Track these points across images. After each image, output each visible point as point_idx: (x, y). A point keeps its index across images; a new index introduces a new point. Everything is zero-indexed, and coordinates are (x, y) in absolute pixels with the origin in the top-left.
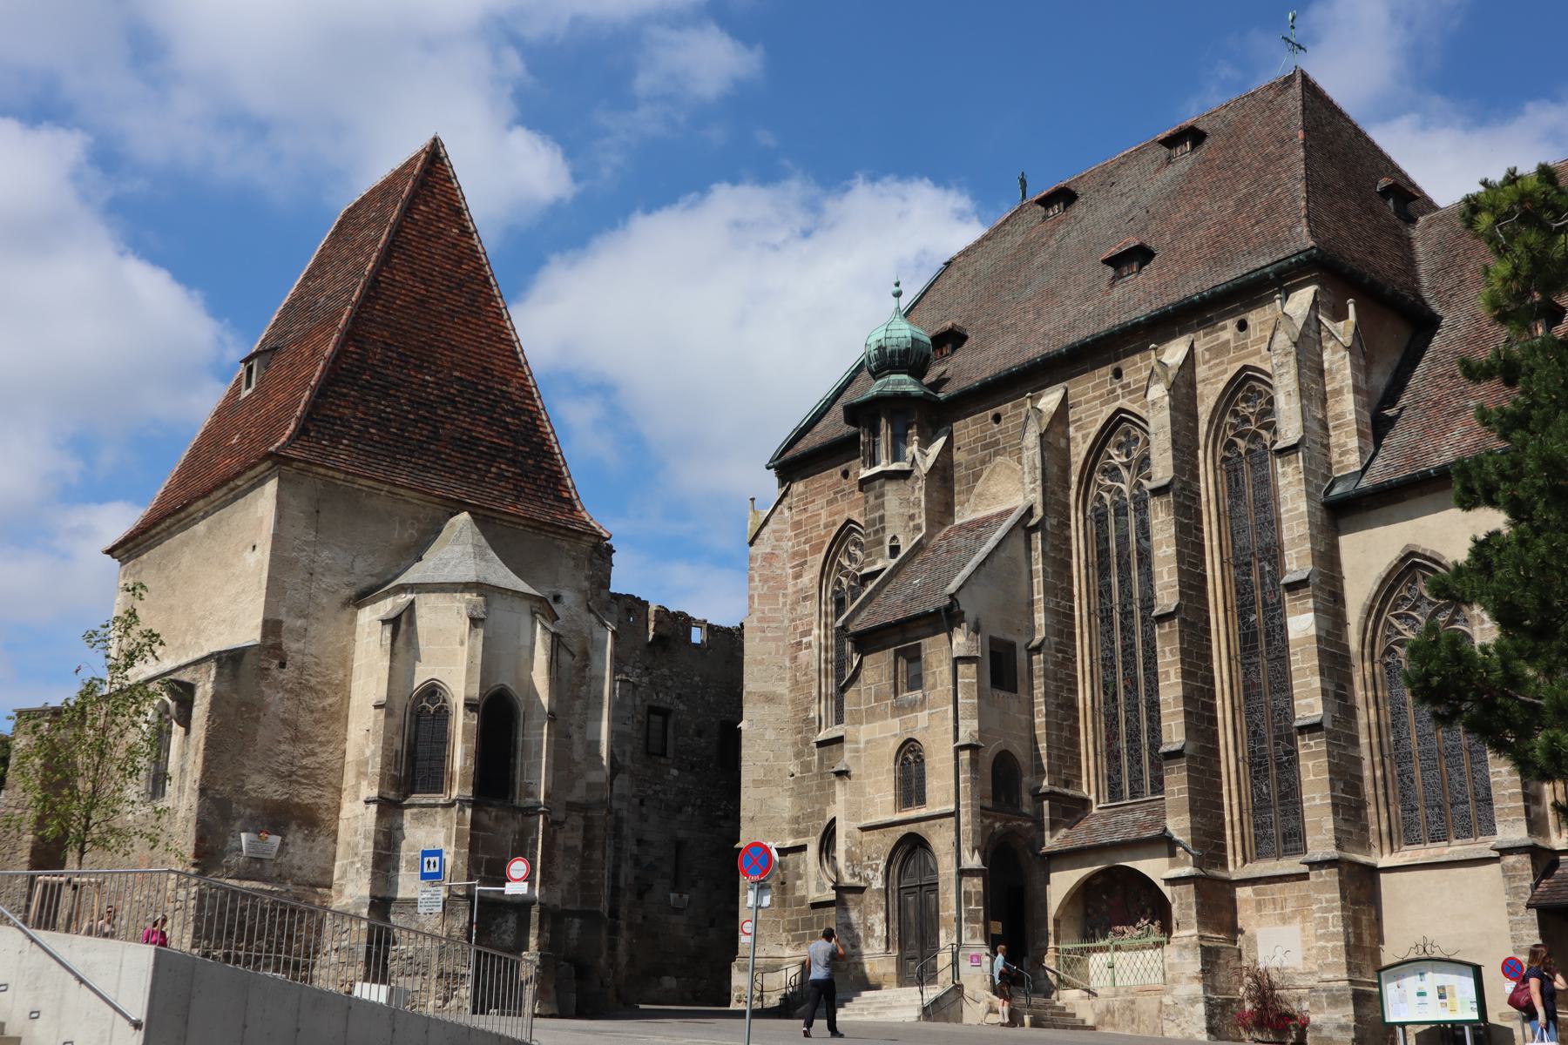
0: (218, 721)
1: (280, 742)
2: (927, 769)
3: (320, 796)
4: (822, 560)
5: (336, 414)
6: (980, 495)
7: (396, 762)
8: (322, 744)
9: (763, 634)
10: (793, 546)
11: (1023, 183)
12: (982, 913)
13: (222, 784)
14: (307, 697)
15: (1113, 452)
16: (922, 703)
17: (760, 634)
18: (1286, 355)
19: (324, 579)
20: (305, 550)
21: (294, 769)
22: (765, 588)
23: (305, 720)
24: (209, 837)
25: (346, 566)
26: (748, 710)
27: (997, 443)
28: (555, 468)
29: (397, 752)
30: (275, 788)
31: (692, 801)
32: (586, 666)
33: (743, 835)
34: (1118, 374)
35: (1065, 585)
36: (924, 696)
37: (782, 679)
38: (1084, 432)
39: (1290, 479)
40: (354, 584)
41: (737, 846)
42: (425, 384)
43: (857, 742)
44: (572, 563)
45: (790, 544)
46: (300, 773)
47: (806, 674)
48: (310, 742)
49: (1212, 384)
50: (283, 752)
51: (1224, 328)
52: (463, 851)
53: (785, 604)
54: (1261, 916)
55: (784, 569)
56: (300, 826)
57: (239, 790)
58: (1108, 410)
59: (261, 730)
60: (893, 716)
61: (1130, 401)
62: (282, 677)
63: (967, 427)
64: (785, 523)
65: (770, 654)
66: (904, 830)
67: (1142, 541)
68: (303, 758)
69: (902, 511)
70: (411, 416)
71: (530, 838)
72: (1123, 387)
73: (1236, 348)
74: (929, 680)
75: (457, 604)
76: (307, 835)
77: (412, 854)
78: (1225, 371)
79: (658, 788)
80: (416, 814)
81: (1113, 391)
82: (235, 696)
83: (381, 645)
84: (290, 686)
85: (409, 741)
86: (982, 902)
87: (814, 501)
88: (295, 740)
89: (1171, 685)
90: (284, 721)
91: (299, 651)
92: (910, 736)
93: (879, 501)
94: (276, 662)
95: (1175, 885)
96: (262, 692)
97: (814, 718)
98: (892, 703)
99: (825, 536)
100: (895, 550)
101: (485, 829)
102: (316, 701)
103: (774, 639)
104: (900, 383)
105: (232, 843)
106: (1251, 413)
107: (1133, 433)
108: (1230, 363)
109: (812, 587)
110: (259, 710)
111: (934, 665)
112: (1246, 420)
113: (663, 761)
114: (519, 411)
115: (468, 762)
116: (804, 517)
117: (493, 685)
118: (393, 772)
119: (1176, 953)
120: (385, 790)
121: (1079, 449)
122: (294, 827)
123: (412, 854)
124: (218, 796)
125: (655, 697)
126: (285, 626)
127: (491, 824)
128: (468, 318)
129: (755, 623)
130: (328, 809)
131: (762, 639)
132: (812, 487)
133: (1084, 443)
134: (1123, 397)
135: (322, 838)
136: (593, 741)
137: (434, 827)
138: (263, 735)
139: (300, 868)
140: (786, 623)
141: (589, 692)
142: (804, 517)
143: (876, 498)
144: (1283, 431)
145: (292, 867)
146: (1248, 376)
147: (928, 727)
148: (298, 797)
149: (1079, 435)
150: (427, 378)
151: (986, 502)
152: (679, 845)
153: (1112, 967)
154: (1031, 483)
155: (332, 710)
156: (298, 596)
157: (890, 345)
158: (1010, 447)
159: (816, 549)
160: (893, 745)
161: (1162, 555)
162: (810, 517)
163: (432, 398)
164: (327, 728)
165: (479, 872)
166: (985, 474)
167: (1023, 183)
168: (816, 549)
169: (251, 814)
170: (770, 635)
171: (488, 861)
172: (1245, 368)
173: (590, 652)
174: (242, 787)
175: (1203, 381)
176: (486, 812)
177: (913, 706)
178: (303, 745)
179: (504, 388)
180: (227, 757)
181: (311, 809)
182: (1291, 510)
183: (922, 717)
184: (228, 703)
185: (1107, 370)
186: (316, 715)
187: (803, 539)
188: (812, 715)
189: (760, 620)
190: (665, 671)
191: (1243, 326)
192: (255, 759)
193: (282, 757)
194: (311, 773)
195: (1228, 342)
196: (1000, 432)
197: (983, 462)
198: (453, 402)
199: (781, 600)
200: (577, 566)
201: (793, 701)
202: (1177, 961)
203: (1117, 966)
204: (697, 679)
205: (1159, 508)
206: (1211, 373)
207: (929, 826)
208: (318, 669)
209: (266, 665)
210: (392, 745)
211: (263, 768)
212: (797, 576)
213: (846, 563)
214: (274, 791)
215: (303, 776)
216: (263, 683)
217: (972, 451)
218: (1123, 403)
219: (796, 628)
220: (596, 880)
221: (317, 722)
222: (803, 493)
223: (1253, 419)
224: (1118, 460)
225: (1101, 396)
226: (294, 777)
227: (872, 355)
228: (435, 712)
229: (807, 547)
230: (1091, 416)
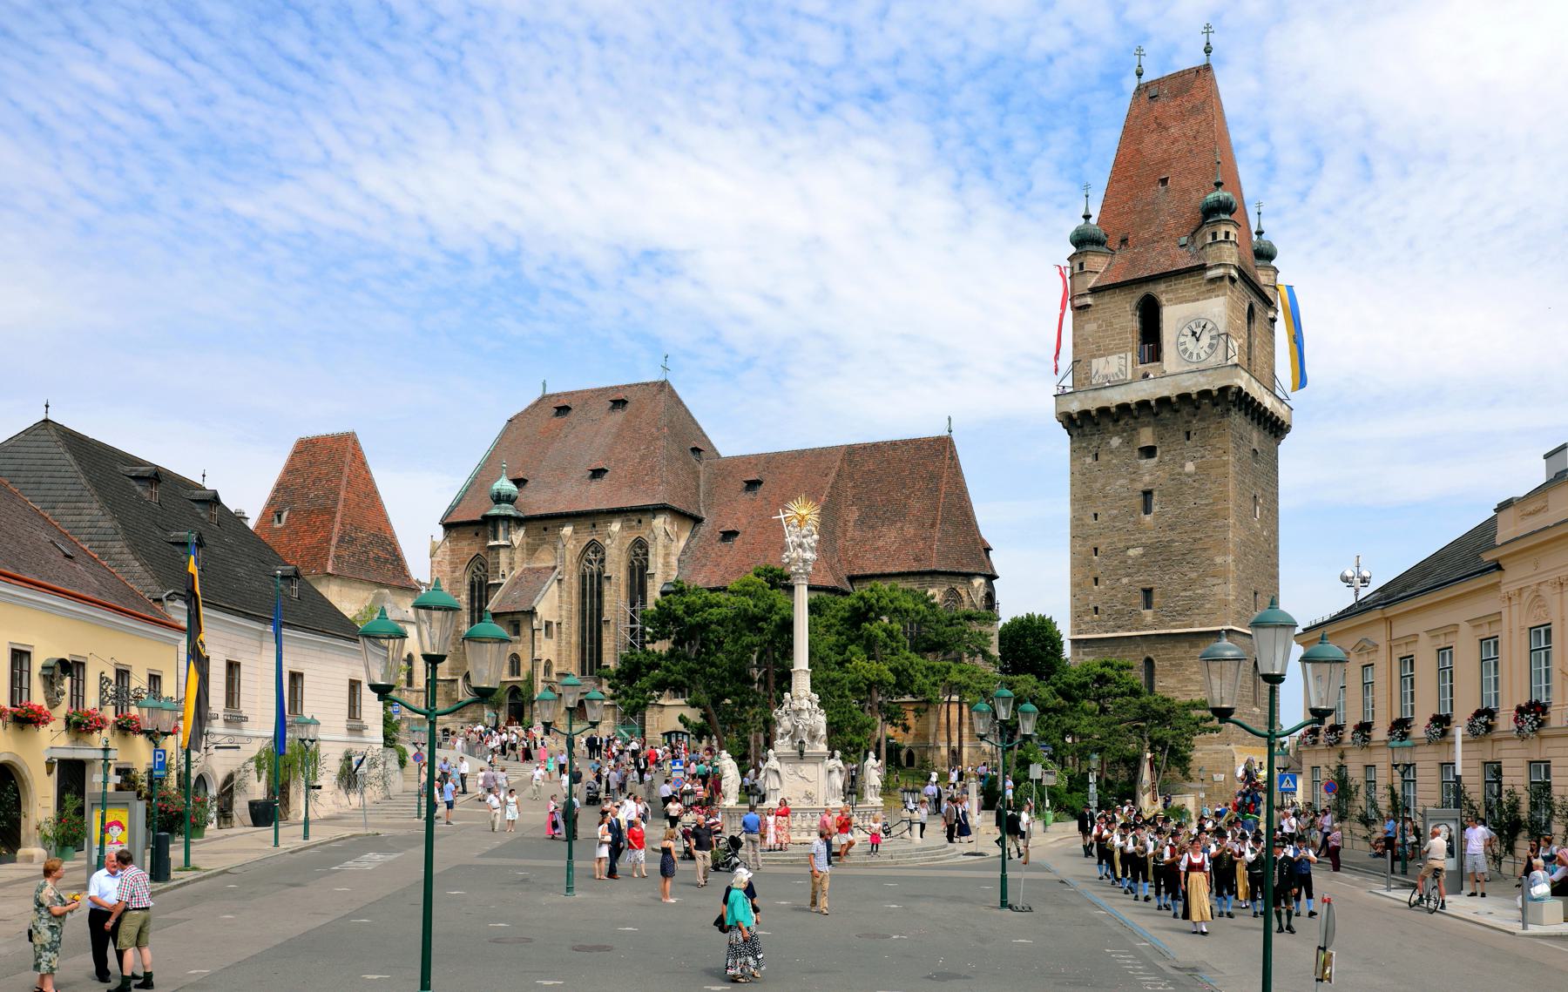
11: (544, 384)
34: (594, 526)
58: (590, 539)
74: (522, 634)
100: (503, 575)
104: (506, 508)
112: (638, 555)
159: (462, 562)
167: (544, 384)
168: (462, 562)
183: (520, 647)
191: (640, 522)
212: (453, 572)
218: (595, 537)
224: (592, 557)
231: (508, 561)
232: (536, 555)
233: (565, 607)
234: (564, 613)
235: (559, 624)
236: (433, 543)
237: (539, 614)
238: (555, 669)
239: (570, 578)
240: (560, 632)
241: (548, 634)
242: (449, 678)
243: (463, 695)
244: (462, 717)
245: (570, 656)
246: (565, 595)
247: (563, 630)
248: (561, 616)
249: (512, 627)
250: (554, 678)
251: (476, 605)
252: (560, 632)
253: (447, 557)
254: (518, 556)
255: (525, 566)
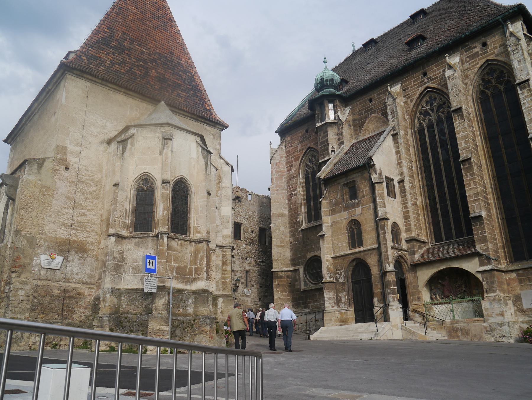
0: (28, 195)
1: (65, 208)
2: (363, 231)
3: (88, 237)
4: (299, 163)
5: (98, 55)
6: (365, 130)
7: (126, 215)
8: (89, 210)
9: (277, 192)
10: (287, 160)
12: (396, 290)
13: (31, 229)
14: (81, 186)
15: (424, 105)
16: (358, 205)
17: (276, 192)
18: (516, 46)
19: (90, 129)
20: (80, 114)
21: (73, 222)
22: (278, 175)
23: (80, 198)
24: (22, 257)
25: (102, 124)
26: (273, 220)
27: (372, 109)
28: (203, 97)
29: (126, 210)
30: (62, 232)
31: (251, 256)
32: (220, 182)
33: (274, 266)
34: (425, 74)
35: (409, 157)
36: (359, 201)
37: (285, 208)
38: (411, 99)
39: (526, 94)
40: (107, 133)
41: (272, 270)
42: (142, 53)
43: (328, 223)
44: (212, 137)
45: (286, 159)
46: (76, 224)
47: (295, 205)
48: (82, 209)
49: (472, 70)
50: (67, 213)
51: (475, 47)
52: (163, 261)
53: (285, 181)
54: (522, 286)
55: (284, 168)
56: (76, 252)
57: (42, 232)
58: (421, 89)
59: (54, 201)
60: (344, 211)
61: (431, 83)
62: (66, 175)
63: (357, 106)
64: (283, 152)
65: (280, 199)
66: (353, 257)
67: (442, 138)
68: (78, 217)
69: (335, 137)
70: (136, 64)
71: (199, 255)
72: (428, 79)
73: (482, 54)
75: (157, 135)
76: (81, 257)
77: (135, 264)
78: (478, 64)
79: (239, 251)
80: (137, 242)
81: (424, 80)
82: (40, 183)
83: (117, 155)
84: (71, 180)
85: (133, 204)
86: (396, 285)
87: (294, 142)
88: (74, 207)
89: (472, 189)
90: (68, 197)
91: (76, 163)
92: (353, 218)
93: (325, 134)
94: (64, 167)
95: (483, 274)
96: (55, 181)
97: (299, 221)
98: (343, 206)
99: (300, 154)
101: (175, 250)
102: (86, 189)
103: (282, 193)
105: (36, 261)
106: (491, 79)
107: (433, 96)
108: (479, 60)
109: (296, 173)
110: (53, 191)
111: (362, 188)
113: (240, 241)
114: (185, 72)
115: (165, 213)
116: (291, 148)
117: (178, 175)
118: (124, 220)
119: (488, 304)
120: (119, 229)
121: (409, 105)
122: (73, 252)
123: (135, 264)
124: (28, 235)
125: (236, 219)
126: (68, 149)
127: (179, 248)
128: (163, 31)
129: (274, 188)
130: (93, 243)
131: (277, 194)
132: (294, 138)
133: (411, 103)
134: (428, 82)
135: (89, 258)
136: (225, 216)
137: (147, 249)
138: (56, 203)
139: (77, 274)
140: (286, 187)
141: (222, 194)
142: (291, 148)
143: (324, 133)
144: (518, 77)
145: (73, 274)
146: (489, 63)
147: (361, 214)
148: (76, 237)
149: (409, 100)
150: (144, 50)
151: (368, 132)
152: (247, 272)
153: (452, 311)
154: (392, 118)
155: (95, 193)
156: (76, 136)
157: (325, 78)
158: (377, 110)
159: (296, 160)
160: (345, 223)
161: (460, 136)
162: (293, 148)
163: (146, 58)
164: (92, 202)
165: (172, 273)
166: (367, 122)
169: (48, 245)
170: (280, 192)
171: (178, 268)
172: (487, 61)
173: (222, 176)
174: (42, 230)
175: (467, 69)
176: (176, 242)
177: (353, 206)
178: (78, 211)
179: (179, 61)
180: (33, 214)
181: (83, 244)
182: (528, 108)
183: (358, 210)
184: (35, 186)
185: (419, 74)
186: (86, 196)
187: (291, 157)
188: (298, 220)
189: (276, 187)
190: (239, 209)
191: (484, 45)
192: (50, 216)
193: (66, 216)
194: (83, 225)
195: (478, 52)
196: (372, 105)
197: (366, 117)
198: (156, 62)
199: (283, 179)
200: (214, 138)
201: (290, 216)
202: (489, 307)
203: (455, 310)
204: (250, 212)
205: (457, 117)
206: (471, 65)
207: (365, 255)
208: (87, 173)
209: (57, 168)
210: (123, 206)
211: (55, 221)
212: (289, 170)
213: (309, 163)
214: (62, 234)
215: (78, 226)
216: (55, 177)
217: (359, 115)
219: (290, 189)
220: (229, 280)
221: (86, 199)
222: (290, 140)
223: (493, 81)
225: (418, 83)
226: (73, 227)
227: (318, 82)
228: (147, 189)
229: (293, 159)
230: (414, 92)
231: (337, 137)
232: (365, 127)
233: (404, 163)
234: (405, 170)
235: (401, 182)
236: (271, 149)
237: (378, 166)
238: (404, 236)
239: (406, 134)
240: (403, 191)
241: (391, 193)
242: (292, 269)
243: (306, 284)
244: (305, 307)
245: (419, 220)
246: (402, 150)
247: (407, 188)
248: (402, 174)
249: (346, 190)
250: (405, 246)
251: (311, 194)
252: (403, 191)
253: (284, 159)
254: (346, 131)
255: (354, 141)
